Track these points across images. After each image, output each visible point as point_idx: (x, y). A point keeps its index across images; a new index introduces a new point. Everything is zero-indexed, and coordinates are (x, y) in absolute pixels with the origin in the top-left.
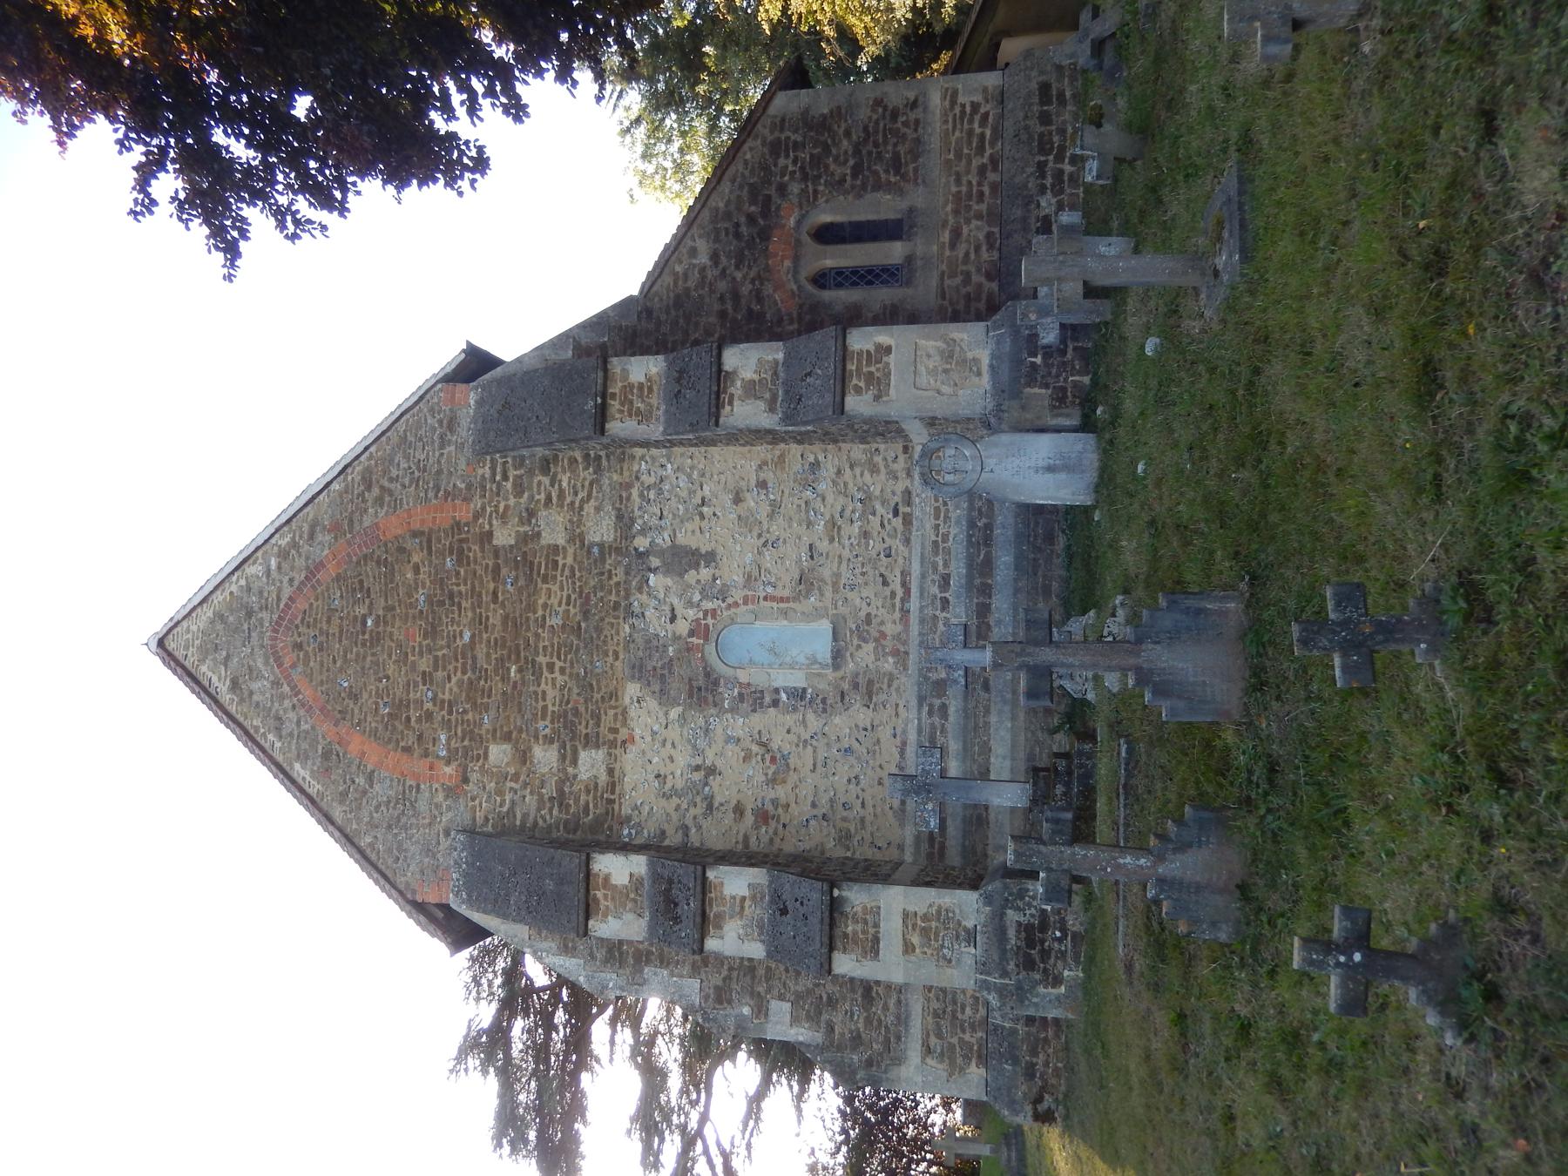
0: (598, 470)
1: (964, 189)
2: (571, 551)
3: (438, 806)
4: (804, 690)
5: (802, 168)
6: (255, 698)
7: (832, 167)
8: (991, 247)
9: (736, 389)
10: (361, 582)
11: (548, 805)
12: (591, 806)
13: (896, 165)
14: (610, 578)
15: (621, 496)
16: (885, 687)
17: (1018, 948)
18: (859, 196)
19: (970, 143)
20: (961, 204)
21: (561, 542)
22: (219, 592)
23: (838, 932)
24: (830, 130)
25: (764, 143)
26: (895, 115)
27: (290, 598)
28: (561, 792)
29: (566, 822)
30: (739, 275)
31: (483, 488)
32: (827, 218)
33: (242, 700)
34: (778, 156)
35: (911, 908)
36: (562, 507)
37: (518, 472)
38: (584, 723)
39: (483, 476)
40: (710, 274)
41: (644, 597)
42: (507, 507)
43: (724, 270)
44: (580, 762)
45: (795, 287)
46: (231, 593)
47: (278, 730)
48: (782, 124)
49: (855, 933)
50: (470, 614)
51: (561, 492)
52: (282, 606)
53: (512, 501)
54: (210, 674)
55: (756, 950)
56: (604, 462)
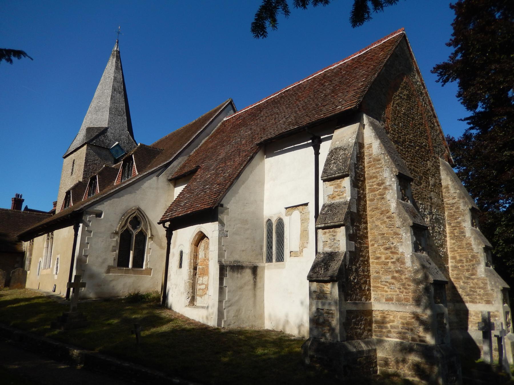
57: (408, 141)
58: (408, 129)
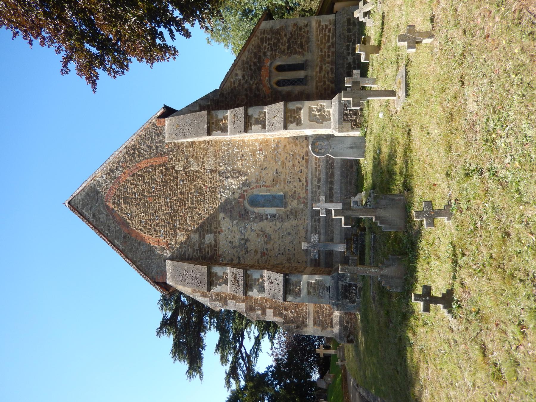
1: (323, 54)
4: (275, 215)
5: (271, 47)
6: (101, 220)
7: (281, 46)
8: (332, 73)
12: (210, 251)
13: (301, 46)
16: (301, 213)
17: (342, 292)
18: (290, 56)
19: (325, 39)
20: (322, 59)
23: (288, 289)
24: (280, 34)
25: (258, 38)
26: (301, 29)
28: (200, 248)
29: (202, 257)
30: (251, 82)
32: (279, 63)
33: (96, 221)
40: (242, 82)
43: (247, 81)
47: (109, 230)
48: (264, 32)
49: (293, 289)
54: (86, 213)
57: (169, 210)
58: (156, 207)
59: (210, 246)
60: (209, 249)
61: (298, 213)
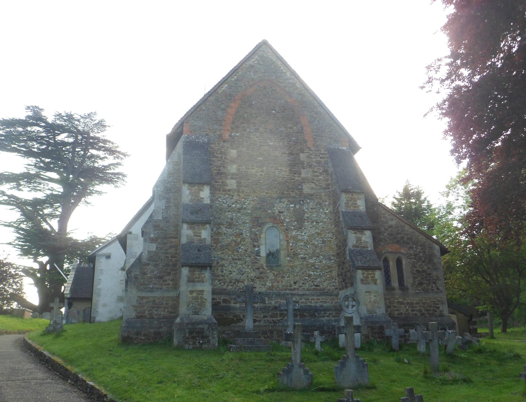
0: (325, 188)
1: (415, 305)
2: (299, 179)
3: (215, 132)
4: (259, 256)
5: (418, 254)
6: (248, 73)
7: (419, 264)
8: (398, 314)
9: (359, 235)
10: (286, 110)
11: (217, 169)
12: (218, 184)
14: (292, 192)
15: (317, 195)
16: (261, 283)
20: (411, 304)
21: (302, 176)
22: (281, 63)
27: (280, 86)
28: (222, 173)
30: (386, 234)
31: (318, 151)
32: (404, 262)
34: (421, 247)
35: (205, 293)
36: (313, 176)
37: (323, 162)
38: (245, 182)
39: (322, 151)
41: (286, 203)
42: (312, 158)
43: (387, 230)
44: (232, 180)
45: (383, 252)
46: (281, 67)
48: (431, 248)
50: (278, 145)
51: (318, 176)
52: (278, 83)
53: (314, 160)
54: (255, 58)
55: (184, 240)
56: (327, 190)
59: (224, 184)
60: (220, 183)
61: (262, 280)
